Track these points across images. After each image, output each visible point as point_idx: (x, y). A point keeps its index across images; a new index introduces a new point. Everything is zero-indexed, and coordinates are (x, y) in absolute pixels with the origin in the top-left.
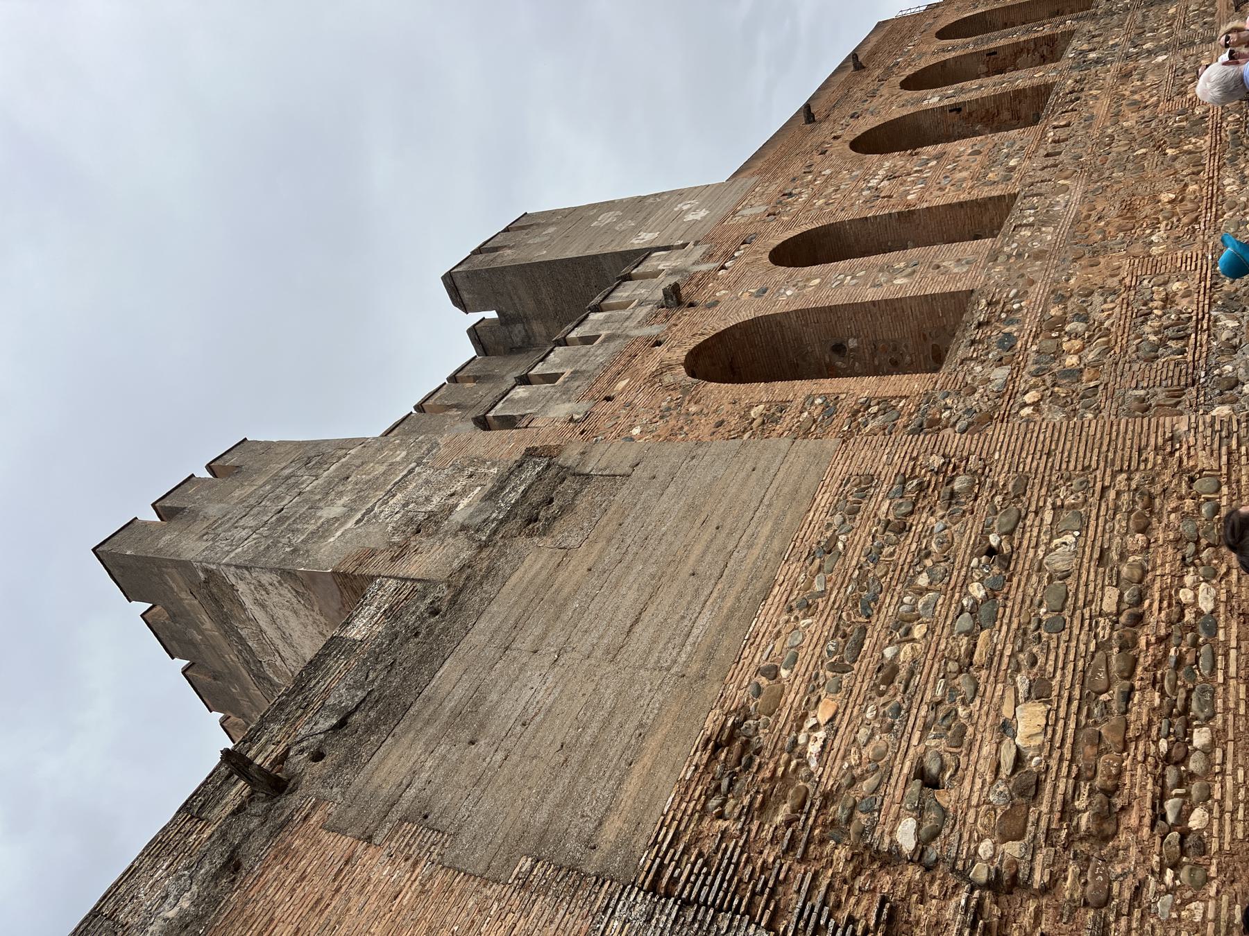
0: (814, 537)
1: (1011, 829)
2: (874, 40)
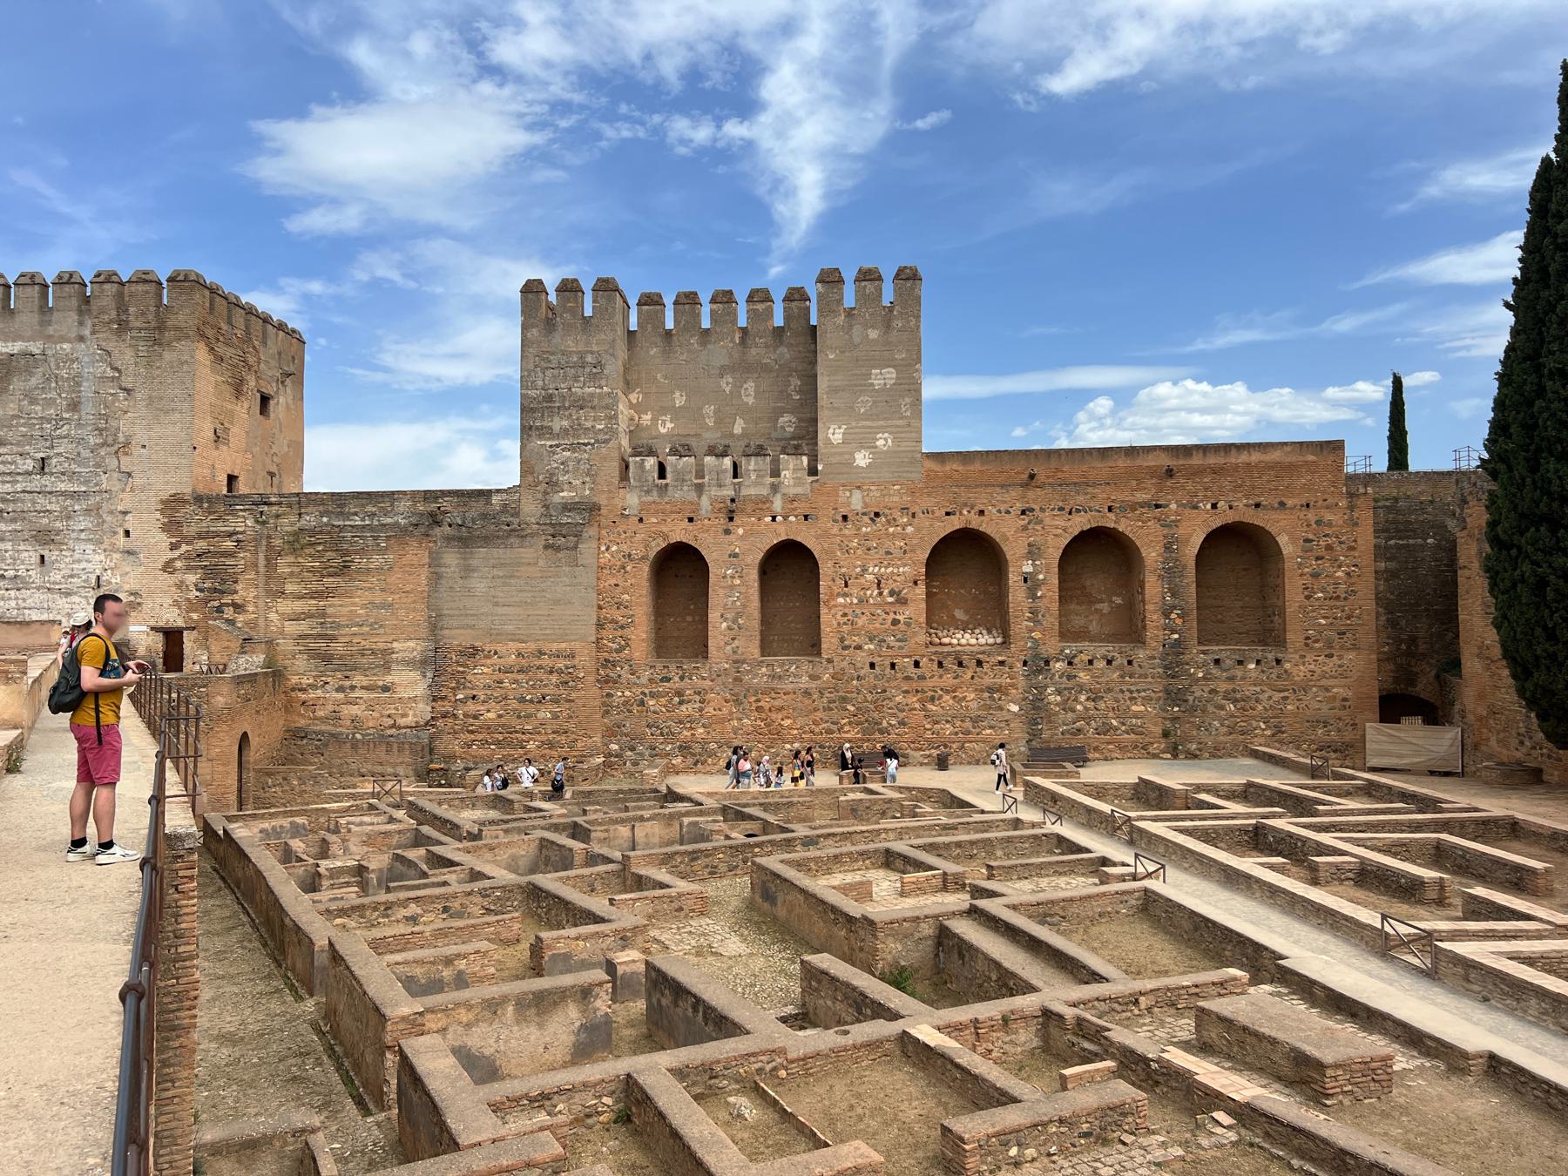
1: (466, 715)
2: (1275, 456)
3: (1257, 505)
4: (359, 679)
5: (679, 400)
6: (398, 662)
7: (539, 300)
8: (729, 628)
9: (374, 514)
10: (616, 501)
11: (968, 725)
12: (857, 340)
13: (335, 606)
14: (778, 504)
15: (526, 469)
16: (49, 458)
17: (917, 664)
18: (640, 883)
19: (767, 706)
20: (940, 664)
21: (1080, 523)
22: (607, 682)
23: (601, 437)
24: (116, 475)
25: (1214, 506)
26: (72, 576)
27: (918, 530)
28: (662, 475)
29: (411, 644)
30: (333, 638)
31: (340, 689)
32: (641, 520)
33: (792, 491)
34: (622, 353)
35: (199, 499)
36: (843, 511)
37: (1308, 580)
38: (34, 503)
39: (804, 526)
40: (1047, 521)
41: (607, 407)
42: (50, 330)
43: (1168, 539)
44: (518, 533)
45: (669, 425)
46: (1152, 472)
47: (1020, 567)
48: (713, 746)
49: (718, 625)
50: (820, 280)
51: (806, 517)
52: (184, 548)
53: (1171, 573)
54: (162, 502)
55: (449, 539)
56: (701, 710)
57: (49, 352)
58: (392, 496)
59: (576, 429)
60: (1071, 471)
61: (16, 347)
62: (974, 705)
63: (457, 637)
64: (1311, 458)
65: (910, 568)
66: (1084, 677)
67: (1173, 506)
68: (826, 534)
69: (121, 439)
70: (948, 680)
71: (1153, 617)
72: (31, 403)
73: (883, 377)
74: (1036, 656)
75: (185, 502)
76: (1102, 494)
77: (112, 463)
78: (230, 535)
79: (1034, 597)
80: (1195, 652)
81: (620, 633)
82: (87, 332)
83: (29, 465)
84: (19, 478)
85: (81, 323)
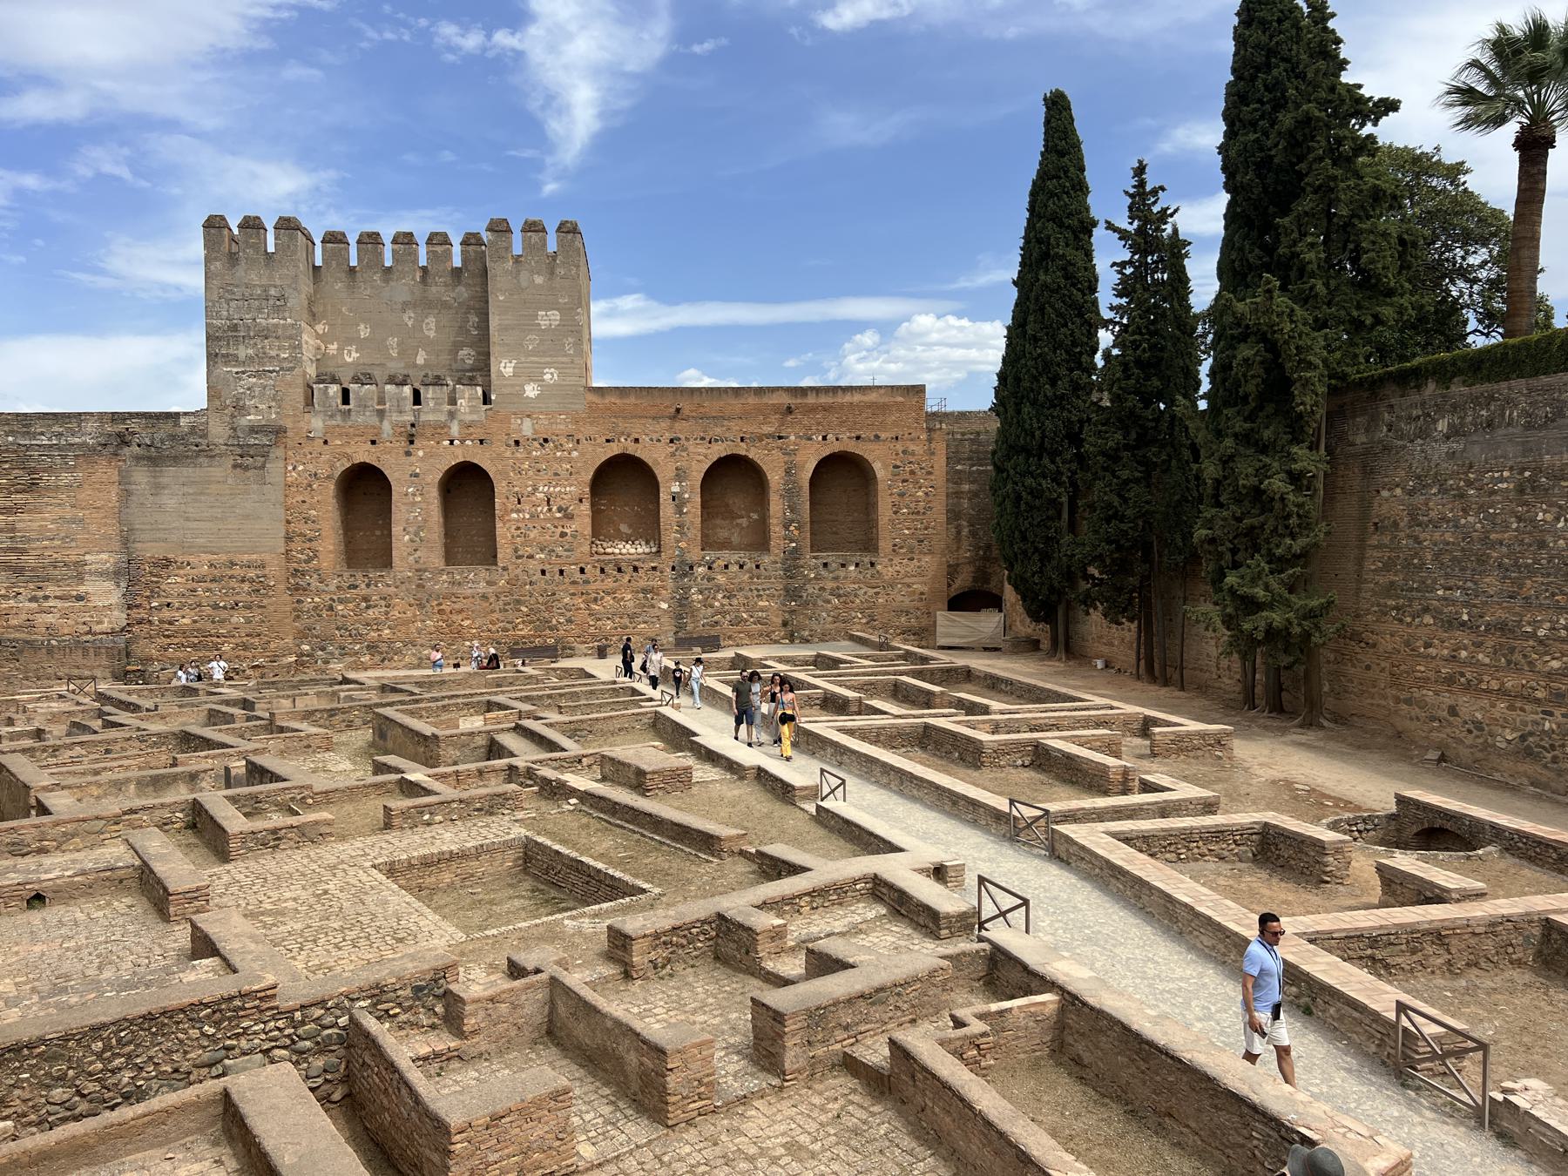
0: (238, 558)
2: (872, 397)
3: (858, 438)
4: (51, 590)
5: (364, 332)
6: (91, 574)
7: (222, 235)
8: (412, 541)
9: (61, 434)
10: (302, 424)
11: (626, 621)
12: (524, 284)
13: (24, 522)
14: (455, 429)
15: (213, 392)
17: (582, 571)
18: (282, 730)
19: (448, 609)
20: (602, 571)
21: (719, 451)
22: (297, 590)
23: (285, 365)
25: (824, 438)
27: (582, 454)
28: (346, 401)
29: (104, 556)
30: (23, 551)
31: (33, 599)
32: (326, 442)
33: (468, 418)
34: (306, 286)
36: (516, 437)
37: (896, 499)
39: (479, 449)
40: (691, 449)
41: (290, 337)
43: (789, 463)
44: (209, 453)
45: (355, 355)
46: (776, 409)
47: (670, 487)
48: (399, 645)
49: (401, 538)
50: (489, 229)
51: (481, 442)
53: (790, 493)
55: (138, 458)
56: (387, 613)
58: (79, 417)
59: (262, 357)
60: (711, 406)
62: (630, 604)
63: (150, 550)
64: (900, 399)
65: (575, 488)
66: (721, 579)
67: (792, 438)
68: (500, 457)
70: (609, 583)
71: (776, 530)
73: (549, 318)
74: (682, 562)
76: (736, 427)
79: (681, 513)
80: (809, 558)
81: (308, 545)
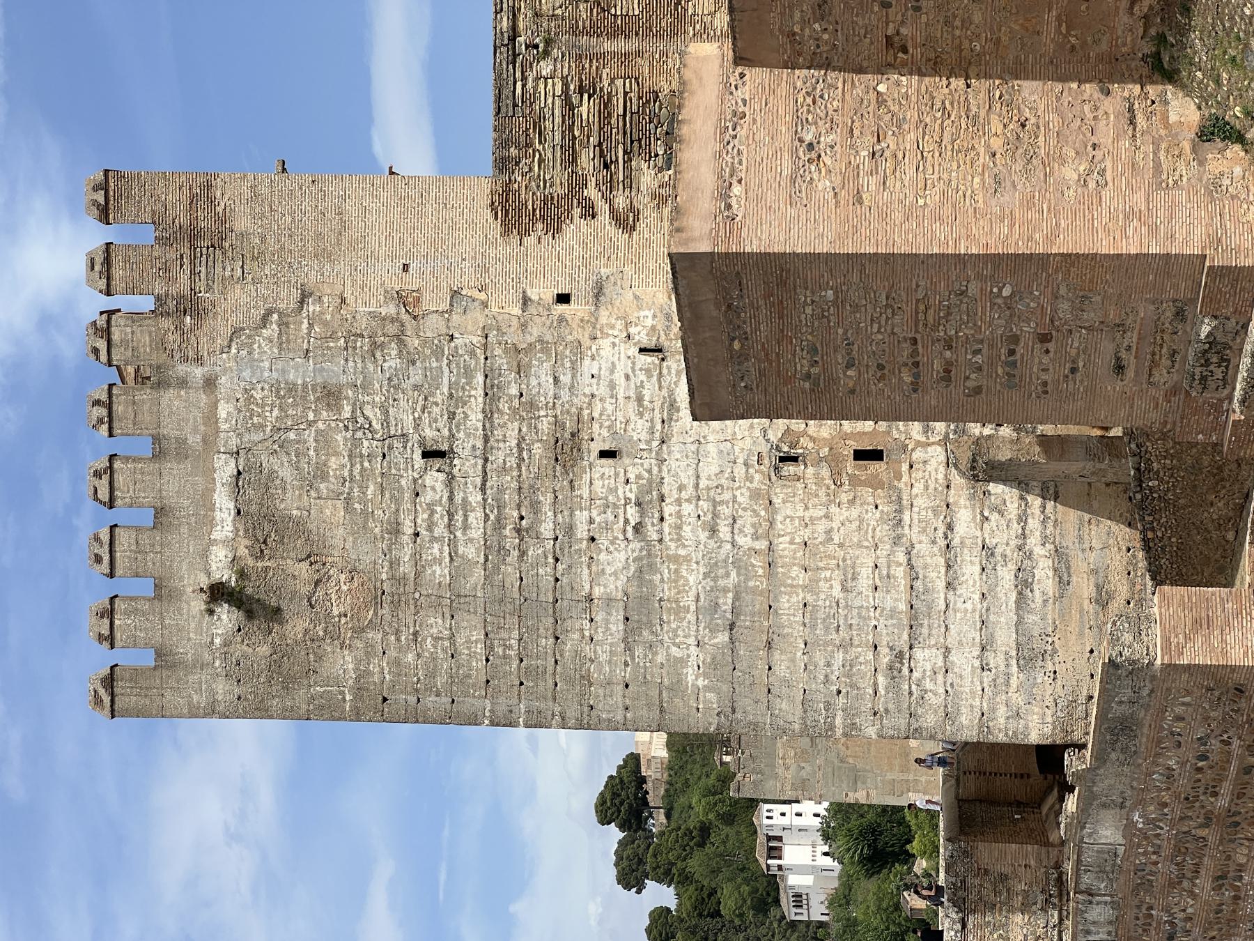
16: (422, 442)
24: (456, 318)
26: (640, 399)
35: (503, 164)
38: (504, 470)
42: (194, 440)
52: (591, 192)
54: (506, 232)
57: (234, 442)
61: (224, 504)
69: (390, 309)
72: (324, 477)
75: (507, 191)
77: (433, 326)
78: (569, 106)
82: (198, 372)
83: (435, 479)
84: (459, 497)
85: (183, 383)
